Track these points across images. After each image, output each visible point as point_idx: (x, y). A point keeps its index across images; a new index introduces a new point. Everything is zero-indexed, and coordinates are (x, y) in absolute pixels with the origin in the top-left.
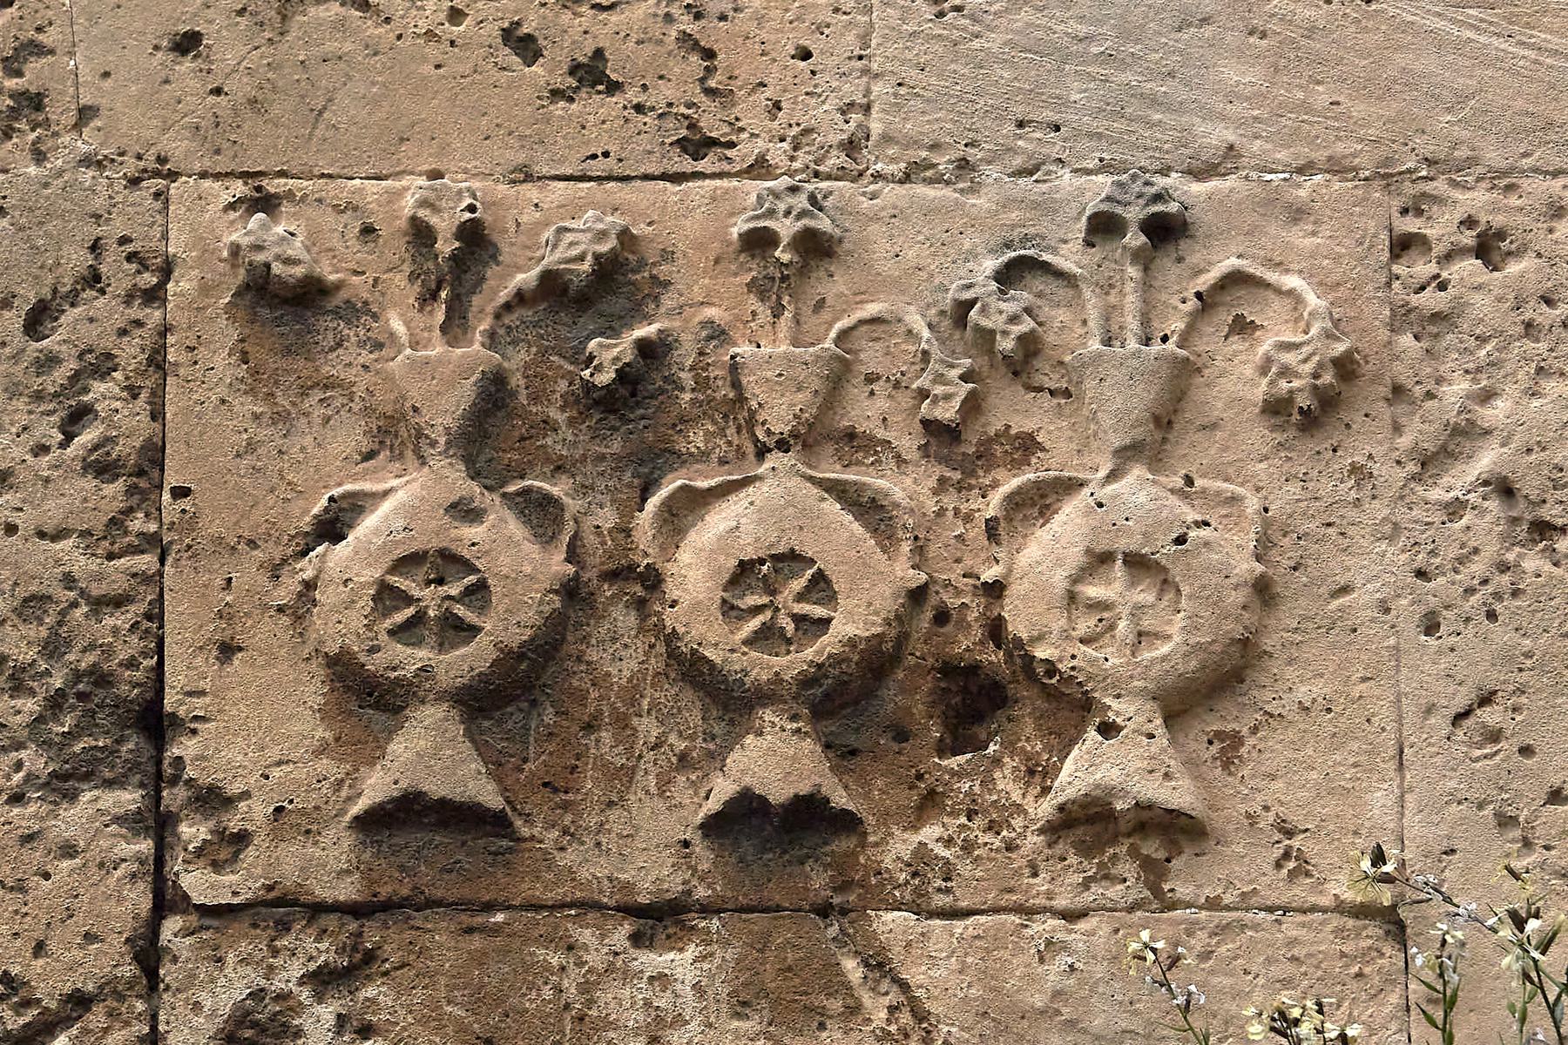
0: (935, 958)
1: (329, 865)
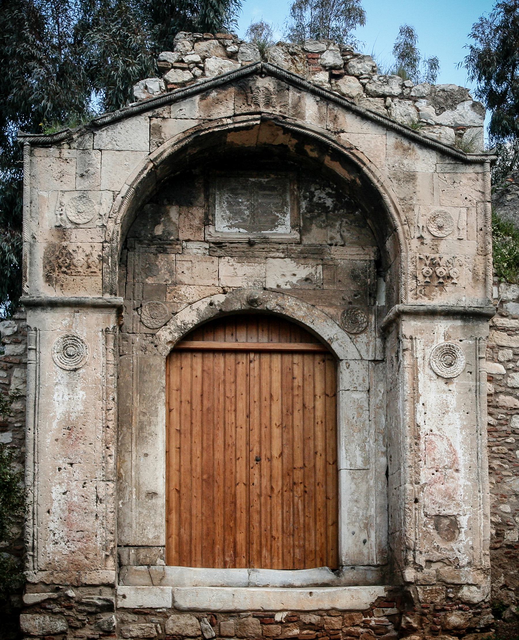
1: (423, 284)
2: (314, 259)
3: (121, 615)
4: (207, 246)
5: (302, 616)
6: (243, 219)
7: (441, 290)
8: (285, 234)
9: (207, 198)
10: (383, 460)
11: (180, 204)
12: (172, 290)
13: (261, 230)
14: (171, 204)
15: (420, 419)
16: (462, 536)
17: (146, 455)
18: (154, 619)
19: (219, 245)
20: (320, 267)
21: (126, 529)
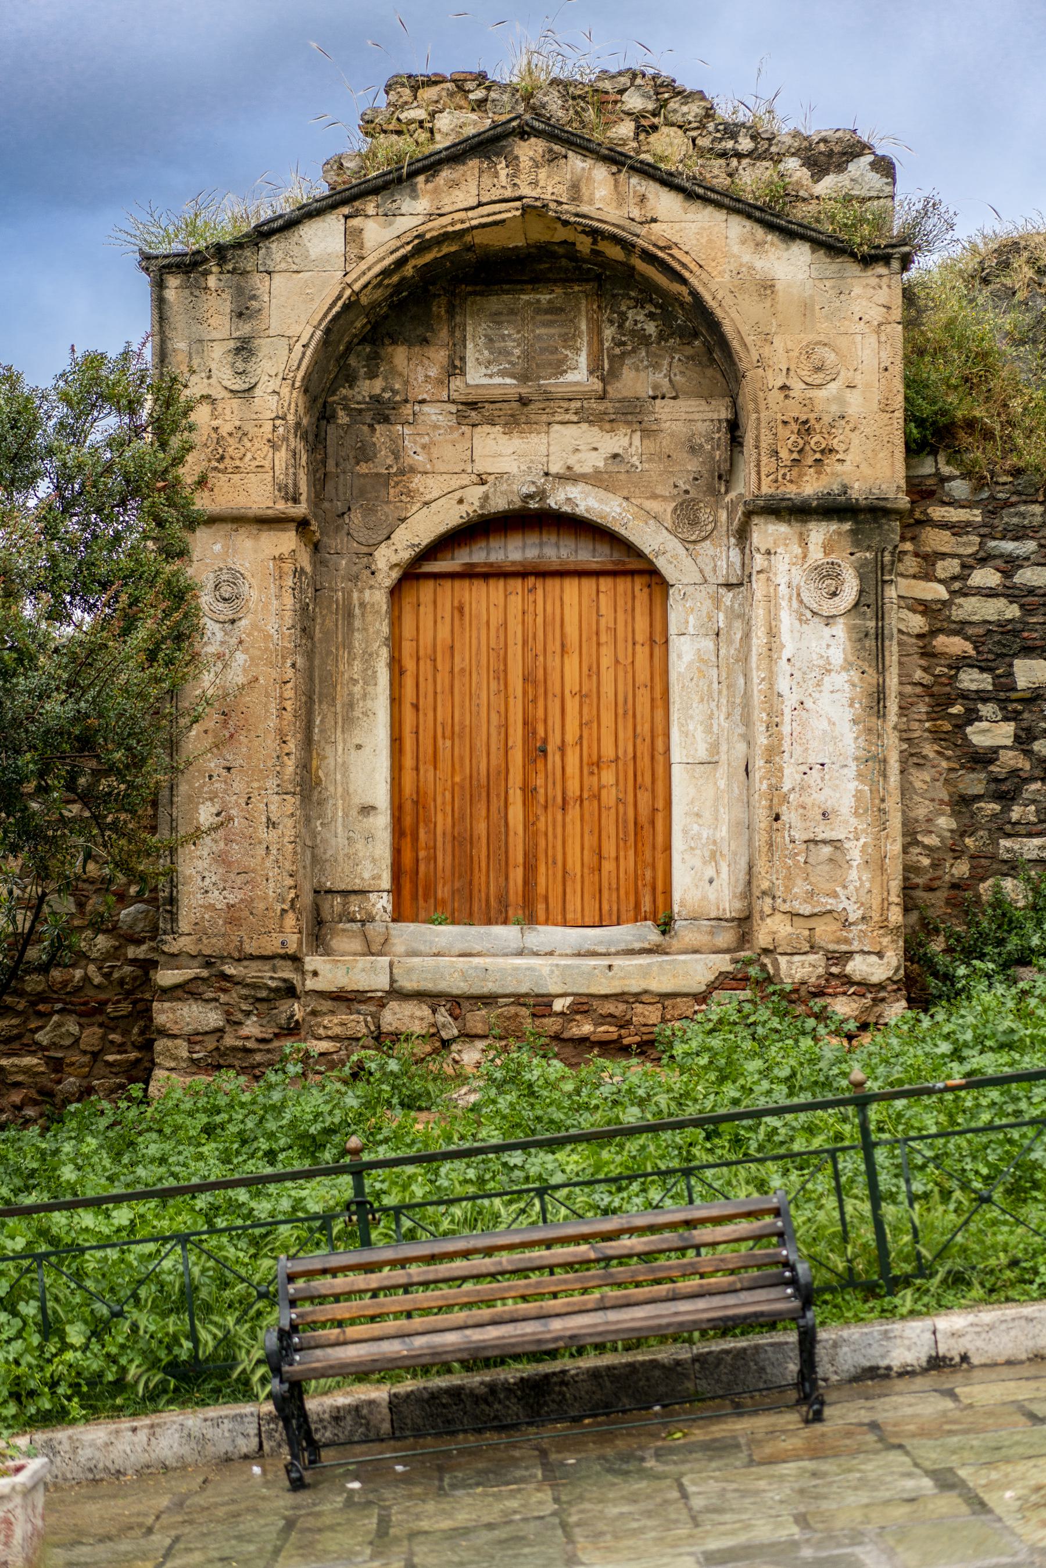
0: (828, 469)
2: (629, 423)
3: (313, 1004)
4: (453, 408)
5: (595, 1003)
6: (510, 362)
7: (819, 473)
8: (577, 384)
9: (452, 333)
10: (741, 747)
11: (409, 343)
12: (397, 484)
13: (539, 378)
14: (394, 342)
15: (783, 685)
16: (853, 874)
17: (359, 747)
18: (363, 1007)
19: (473, 405)
20: (637, 436)
21: (328, 865)
